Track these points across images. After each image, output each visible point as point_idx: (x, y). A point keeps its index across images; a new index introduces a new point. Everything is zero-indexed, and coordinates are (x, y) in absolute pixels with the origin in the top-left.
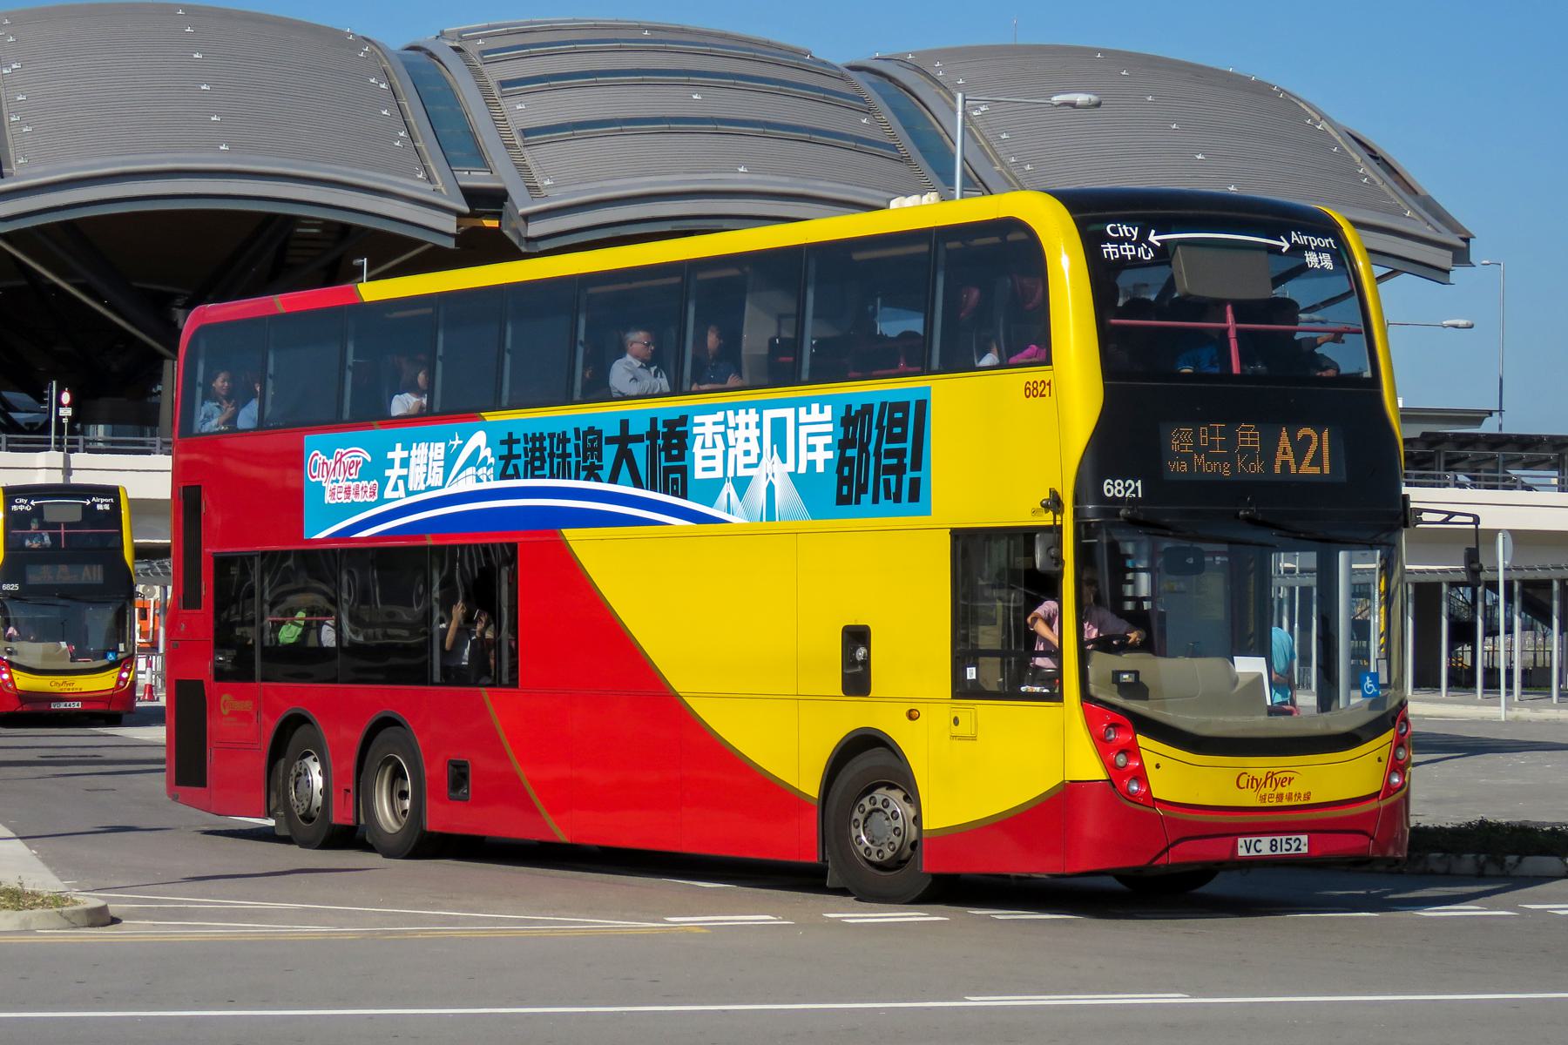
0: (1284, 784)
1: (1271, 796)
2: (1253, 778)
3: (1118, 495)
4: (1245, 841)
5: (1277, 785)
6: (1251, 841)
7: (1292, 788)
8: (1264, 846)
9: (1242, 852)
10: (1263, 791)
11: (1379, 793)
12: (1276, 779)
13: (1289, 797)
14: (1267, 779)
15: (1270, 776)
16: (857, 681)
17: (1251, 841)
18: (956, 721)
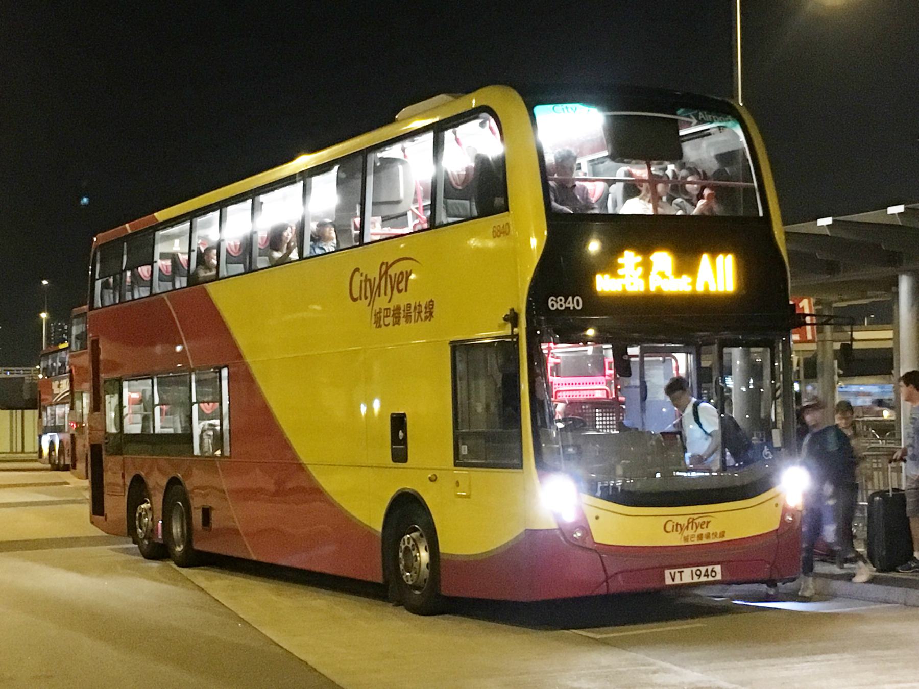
0: (703, 526)
1: (693, 536)
2: (677, 524)
3: (560, 308)
4: (671, 573)
5: (697, 528)
6: (675, 573)
7: (711, 529)
8: (687, 576)
9: (668, 581)
10: (686, 533)
11: (777, 530)
12: (696, 523)
13: (708, 536)
14: (689, 523)
15: (691, 522)
16: (400, 454)
17: (675, 573)
18: (458, 483)
